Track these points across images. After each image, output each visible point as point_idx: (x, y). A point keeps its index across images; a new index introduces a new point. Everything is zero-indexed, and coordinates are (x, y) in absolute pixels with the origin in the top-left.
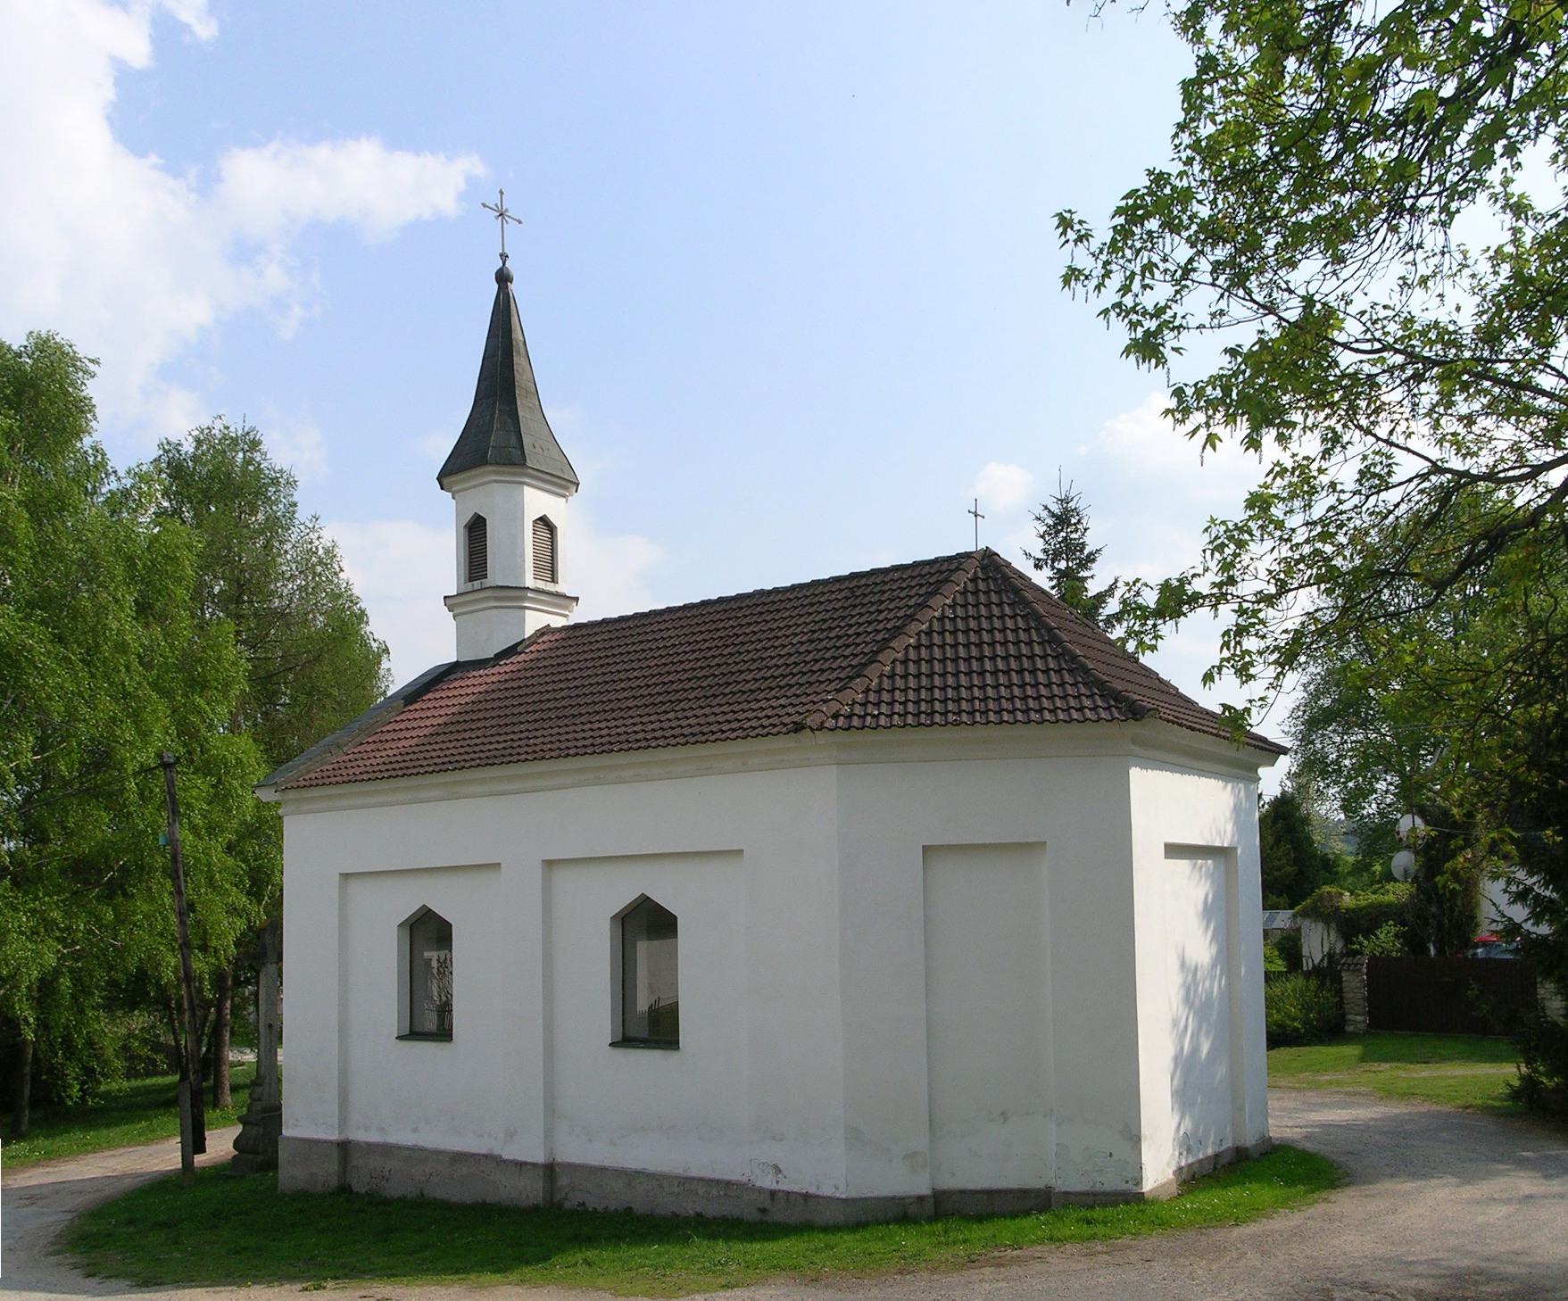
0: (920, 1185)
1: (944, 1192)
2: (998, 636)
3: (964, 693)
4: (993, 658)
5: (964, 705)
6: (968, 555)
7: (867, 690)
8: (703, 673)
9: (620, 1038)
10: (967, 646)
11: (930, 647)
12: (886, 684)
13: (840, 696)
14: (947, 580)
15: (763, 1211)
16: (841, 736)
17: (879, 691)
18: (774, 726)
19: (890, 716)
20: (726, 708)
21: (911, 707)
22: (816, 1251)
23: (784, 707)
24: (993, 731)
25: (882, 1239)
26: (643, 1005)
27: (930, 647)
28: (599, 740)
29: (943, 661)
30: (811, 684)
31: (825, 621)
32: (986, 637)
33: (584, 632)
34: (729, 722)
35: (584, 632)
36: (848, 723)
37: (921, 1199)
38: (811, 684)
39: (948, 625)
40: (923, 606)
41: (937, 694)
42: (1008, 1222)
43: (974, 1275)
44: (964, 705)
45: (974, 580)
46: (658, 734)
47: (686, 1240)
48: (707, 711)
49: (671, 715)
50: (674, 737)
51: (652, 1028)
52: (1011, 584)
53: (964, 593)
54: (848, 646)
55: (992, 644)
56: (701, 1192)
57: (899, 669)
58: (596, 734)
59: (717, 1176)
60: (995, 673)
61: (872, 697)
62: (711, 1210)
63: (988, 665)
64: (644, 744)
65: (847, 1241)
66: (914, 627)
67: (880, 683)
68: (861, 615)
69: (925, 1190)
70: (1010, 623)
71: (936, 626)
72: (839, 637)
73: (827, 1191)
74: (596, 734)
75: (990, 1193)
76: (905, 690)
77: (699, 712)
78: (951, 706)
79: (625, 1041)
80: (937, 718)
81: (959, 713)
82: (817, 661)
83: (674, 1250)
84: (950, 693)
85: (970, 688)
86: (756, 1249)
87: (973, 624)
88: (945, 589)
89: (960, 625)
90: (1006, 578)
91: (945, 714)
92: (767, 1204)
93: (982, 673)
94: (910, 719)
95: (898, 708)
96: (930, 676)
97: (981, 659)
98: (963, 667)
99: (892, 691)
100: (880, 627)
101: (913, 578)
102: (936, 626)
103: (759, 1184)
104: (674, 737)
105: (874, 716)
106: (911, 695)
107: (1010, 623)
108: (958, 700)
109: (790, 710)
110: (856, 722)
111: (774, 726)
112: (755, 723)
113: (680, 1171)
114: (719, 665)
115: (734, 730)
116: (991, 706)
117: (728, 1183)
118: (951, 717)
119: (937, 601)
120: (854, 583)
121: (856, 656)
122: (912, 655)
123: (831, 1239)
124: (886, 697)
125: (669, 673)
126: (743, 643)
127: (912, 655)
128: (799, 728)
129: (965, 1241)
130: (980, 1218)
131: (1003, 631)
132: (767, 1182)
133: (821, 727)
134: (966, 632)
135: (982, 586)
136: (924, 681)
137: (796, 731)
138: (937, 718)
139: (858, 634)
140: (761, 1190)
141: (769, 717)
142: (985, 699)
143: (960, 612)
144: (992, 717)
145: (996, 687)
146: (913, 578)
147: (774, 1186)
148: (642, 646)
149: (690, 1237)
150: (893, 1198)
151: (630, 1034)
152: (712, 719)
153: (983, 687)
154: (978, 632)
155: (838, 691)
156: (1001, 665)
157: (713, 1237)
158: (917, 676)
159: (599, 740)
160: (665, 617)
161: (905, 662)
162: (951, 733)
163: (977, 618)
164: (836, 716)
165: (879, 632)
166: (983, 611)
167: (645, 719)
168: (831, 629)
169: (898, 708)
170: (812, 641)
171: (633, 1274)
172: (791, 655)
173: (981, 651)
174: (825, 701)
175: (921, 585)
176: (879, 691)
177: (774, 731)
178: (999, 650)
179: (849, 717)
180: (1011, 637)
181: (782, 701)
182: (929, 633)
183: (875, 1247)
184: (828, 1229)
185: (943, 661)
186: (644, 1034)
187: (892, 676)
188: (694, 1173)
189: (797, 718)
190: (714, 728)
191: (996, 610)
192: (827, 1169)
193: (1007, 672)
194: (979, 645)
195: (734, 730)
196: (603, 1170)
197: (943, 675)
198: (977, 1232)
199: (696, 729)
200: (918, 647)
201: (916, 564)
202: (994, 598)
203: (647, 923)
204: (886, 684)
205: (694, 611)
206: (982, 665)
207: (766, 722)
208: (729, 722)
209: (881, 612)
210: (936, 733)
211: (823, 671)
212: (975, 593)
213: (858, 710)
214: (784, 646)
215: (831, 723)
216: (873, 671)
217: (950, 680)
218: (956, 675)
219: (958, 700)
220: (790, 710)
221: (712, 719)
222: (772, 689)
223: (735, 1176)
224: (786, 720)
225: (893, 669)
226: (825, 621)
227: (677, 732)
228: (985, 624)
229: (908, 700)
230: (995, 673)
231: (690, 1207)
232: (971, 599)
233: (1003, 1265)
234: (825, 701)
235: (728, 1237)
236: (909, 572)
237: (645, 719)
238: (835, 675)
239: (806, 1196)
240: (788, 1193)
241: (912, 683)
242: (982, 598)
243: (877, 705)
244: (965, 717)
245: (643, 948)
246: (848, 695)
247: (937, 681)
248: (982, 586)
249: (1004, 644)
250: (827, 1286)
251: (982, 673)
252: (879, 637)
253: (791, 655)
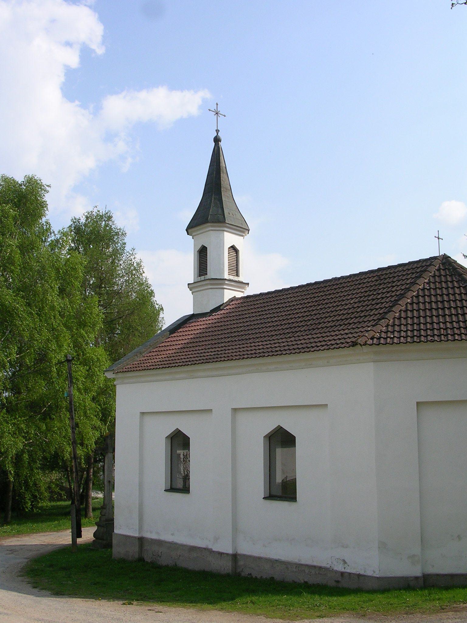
0: (416, 571)
1: (429, 575)
2: (452, 297)
3: (435, 326)
4: (449, 308)
5: (436, 332)
6: (435, 258)
7: (387, 326)
8: (308, 318)
9: (268, 495)
10: (436, 302)
11: (418, 303)
12: (397, 322)
13: (374, 328)
14: (425, 271)
15: (338, 582)
16: (375, 348)
17: (393, 326)
18: (343, 343)
19: (399, 338)
20: (319, 335)
21: (409, 333)
22: (364, 602)
23: (347, 334)
24: (451, 345)
25: (397, 597)
26: (279, 479)
27: (418, 303)
28: (258, 351)
29: (424, 310)
30: (360, 323)
31: (366, 292)
32: (446, 298)
33: (251, 299)
34: (320, 342)
35: (251, 299)
36: (378, 342)
37: (417, 578)
38: (360, 323)
39: (427, 293)
40: (414, 283)
41: (422, 326)
42: (461, 590)
43: (443, 615)
44: (436, 332)
45: (439, 270)
46: (286, 348)
47: (299, 594)
48: (310, 336)
49: (293, 339)
50: (294, 349)
51: (283, 491)
52: (457, 271)
53: (434, 276)
54: (378, 304)
55: (449, 301)
56: (307, 571)
57: (403, 315)
58: (257, 348)
59: (315, 564)
60: (451, 315)
61: (390, 329)
62: (312, 580)
63: (447, 312)
64: (279, 353)
65: (379, 598)
66: (410, 294)
67: (394, 322)
68: (384, 288)
69: (419, 574)
70: (457, 291)
71: (421, 293)
72: (373, 300)
73: (369, 573)
74: (257, 348)
75: (452, 576)
76: (406, 325)
77: (306, 337)
78: (429, 332)
79: (270, 497)
80: (423, 339)
81: (433, 336)
82: (362, 311)
83: (294, 599)
84: (429, 326)
85: (438, 323)
86: (335, 600)
87: (439, 292)
88: (426, 275)
89: (433, 292)
90: (455, 269)
91: (426, 336)
92: (340, 579)
93: (444, 316)
94: (409, 339)
95: (403, 334)
96: (418, 318)
97: (443, 309)
98: (434, 313)
99: (400, 325)
100: (393, 294)
101: (409, 270)
102: (421, 293)
103: (335, 568)
104: (294, 349)
105: (391, 338)
106: (409, 327)
107: (457, 291)
108: (433, 330)
109: (350, 335)
110: (382, 341)
111: (343, 343)
112: (333, 342)
113: (296, 561)
114: (316, 314)
115: (323, 346)
116: (449, 332)
117: (320, 568)
118: (429, 338)
119: (421, 281)
120: (380, 273)
121: (382, 308)
122: (409, 307)
123: (371, 596)
124: (397, 328)
125: (291, 318)
126: (327, 303)
127: (409, 307)
128: (354, 344)
129: (439, 599)
130: (447, 588)
131: (454, 294)
132: (339, 568)
133: (365, 344)
134: (435, 296)
135: (443, 273)
136: (416, 321)
137: (353, 346)
138: (423, 339)
139: (383, 298)
140: (336, 572)
141: (340, 339)
142: (446, 329)
143: (432, 286)
144: (450, 337)
145: (451, 323)
146: (409, 270)
147: (343, 570)
148: (279, 306)
149: (301, 593)
150: (403, 578)
151: (274, 493)
152: (312, 340)
153: (445, 323)
154: (441, 295)
155: (373, 326)
156: (453, 311)
157: (313, 593)
158: (412, 318)
159: (258, 351)
160: (290, 292)
161: (406, 311)
162: (430, 346)
163: (441, 289)
164: (372, 338)
165: (392, 296)
166: (444, 285)
167: (280, 341)
168: (369, 296)
169: (403, 334)
170: (360, 302)
171: (274, 608)
172: (350, 309)
173: (444, 305)
174: (367, 331)
175: (413, 273)
176: (393, 326)
177: (343, 346)
178: (453, 304)
179: (379, 339)
180: (458, 297)
181: (346, 331)
182: (417, 297)
183: (392, 601)
184: (369, 592)
185: (424, 310)
186: (279, 493)
187: (399, 318)
188: (303, 562)
189: (354, 340)
190: (313, 345)
191: (450, 285)
192: (369, 563)
193: (457, 315)
194: (442, 302)
195: (323, 346)
196: (260, 558)
197: (425, 317)
198: (446, 595)
199: (304, 346)
200: (412, 304)
201: (410, 263)
202: (449, 279)
203: (281, 439)
204: (397, 322)
205: (304, 289)
206: (444, 312)
207: (338, 342)
208: (320, 342)
209: (393, 287)
210: (422, 346)
211: (366, 316)
212: (440, 276)
213: (383, 335)
214: (347, 304)
215: (370, 342)
216: (390, 316)
217: (429, 320)
218: (431, 317)
219: (433, 330)
220: (350, 335)
221: (312, 340)
222: (341, 325)
223: (324, 565)
224: (349, 340)
225: (400, 314)
226: (366, 292)
227: (296, 347)
228: (445, 291)
229: (407, 330)
230: (451, 315)
231: (301, 578)
232: (437, 279)
233: (459, 611)
234: (367, 331)
235: (320, 594)
236: (407, 267)
237: (280, 341)
238: (372, 318)
239: (359, 576)
240: (350, 574)
241: (410, 321)
242: (443, 279)
243: (393, 332)
244: (436, 338)
245: (279, 451)
246: (378, 328)
247: (422, 320)
248: (443, 273)
249: (455, 301)
250: (369, 619)
251: (444, 316)
252: (393, 299)
253: (350, 309)
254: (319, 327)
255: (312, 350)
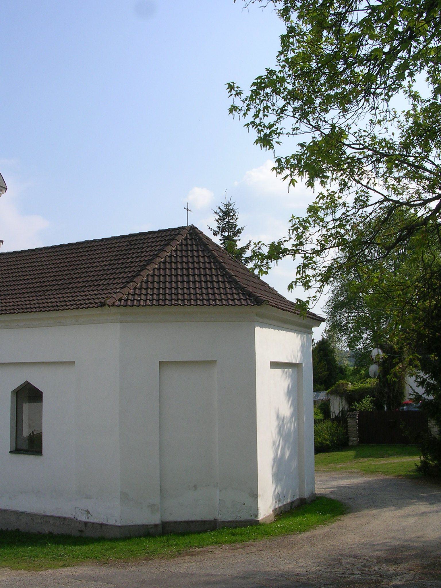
0: (155, 519)
1: (167, 523)
2: (196, 265)
3: (180, 291)
4: (194, 275)
5: (180, 297)
6: (183, 228)
7: (135, 288)
8: (59, 278)
9: (14, 449)
10: (182, 269)
11: (165, 269)
12: (144, 285)
13: (122, 291)
14: (173, 239)
15: (81, 531)
16: (123, 310)
17: (141, 289)
18: (91, 303)
19: (145, 301)
20: (69, 295)
21: (155, 297)
22: (106, 550)
23: (96, 295)
24: (192, 309)
25: (137, 544)
26: (26, 433)
27: (165, 269)
28: (9, 308)
29: (170, 276)
30: (109, 284)
31: (117, 255)
32: (191, 266)
33: (5, 257)
34: (70, 301)
35: (5, 257)
36: (126, 303)
37: (156, 526)
38: (109, 284)
39: (173, 260)
40: (162, 250)
41: (167, 291)
42: (197, 536)
43: (180, 560)
44: (180, 297)
45: (186, 239)
46: (37, 306)
47: (44, 545)
48: (60, 296)
49: (43, 297)
50: (44, 307)
51: (30, 444)
52: (202, 242)
53: (181, 245)
54: (127, 268)
55: (193, 269)
56: (52, 522)
57: (150, 279)
58: (8, 304)
59: (59, 515)
60: (194, 282)
61: (137, 292)
62: (57, 531)
63: (191, 278)
64: (30, 310)
65: (121, 545)
66: (158, 260)
67: (141, 285)
68: (134, 253)
69: (158, 521)
70: (202, 260)
71: (168, 260)
72: (123, 263)
73: (111, 522)
74: (8, 304)
75: (188, 523)
76: (153, 289)
77: (56, 296)
78: (174, 297)
79: (17, 450)
80: (167, 302)
81: (177, 300)
82: (112, 274)
83: (39, 549)
84: (173, 291)
85: (183, 289)
86: (78, 549)
87: (185, 259)
88: (173, 243)
89: (179, 259)
90: (200, 239)
91: (171, 300)
92: (83, 528)
93: (188, 282)
94: (155, 302)
95: (149, 297)
96: (164, 282)
97: (188, 276)
98: (180, 279)
99: (146, 289)
100: (142, 259)
101: (158, 237)
102: (168, 260)
103: (79, 519)
104: (44, 307)
105: (138, 300)
106: (156, 291)
107: (202, 260)
108: (177, 294)
109: (99, 296)
110: (129, 303)
111: (91, 303)
112: (82, 302)
113: (42, 512)
114: (67, 275)
115: (72, 305)
116: (192, 297)
117: (65, 519)
118: (174, 302)
119: (169, 248)
120: (131, 239)
121: (130, 272)
122: (157, 272)
123: (113, 544)
124: (144, 292)
125: (43, 277)
126: (78, 265)
127: (157, 272)
128: (103, 305)
129: (176, 545)
130: (183, 534)
131: (199, 263)
132: (83, 518)
133: (113, 305)
134: (181, 263)
135: (189, 242)
136: (162, 285)
137: (101, 306)
138: (167, 302)
139: (132, 262)
140: (80, 522)
141: (89, 299)
142: (190, 294)
143: (179, 253)
144: (193, 302)
145: (195, 289)
146: (158, 237)
147: (86, 520)
148: (32, 264)
149: (46, 543)
150: (143, 525)
151: (19, 447)
152: (62, 299)
153: (189, 289)
154: (187, 263)
155: (122, 288)
156: (197, 278)
157: (57, 543)
158: (159, 283)
159: (9, 308)
161: (153, 276)
162: (174, 309)
163: (187, 257)
164: (120, 300)
165: (141, 261)
166: (190, 253)
167: (31, 299)
168: (119, 259)
169: (149, 297)
170: (110, 265)
171: (19, 560)
172: (100, 271)
173: (188, 272)
174: (116, 293)
175: (162, 241)
176: (141, 289)
177: (91, 306)
178: (197, 272)
179: (126, 300)
180: (202, 266)
181: (95, 292)
182: (165, 263)
183: (133, 548)
184: (111, 540)
185: (170, 276)
186: (25, 446)
187: (147, 282)
188: (48, 514)
189: (102, 300)
190: (63, 304)
191: (195, 254)
192: (110, 511)
193: (200, 282)
194: (187, 269)
195: (72, 305)
196: (6, 511)
197: (170, 282)
198: (182, 540)
199: (55, 304)
200: (159, 269)
201: (160, 231)
202: (195, 248)
203: (28, 395)
204: (144, 285)
205: (57, 249)
206: (189, 278)
207: (87, 302)
208: (70, 301)
209: (142, 252)
210: (167, 309)
211: (115, 279)
212: (186, 245)
213: (131, 297)
214: (97, 267)
215: (118, 303)
216: (138, 279)
217: (174, 285)
218: (176, 283)
219: (177, 294)
220: (99, 296)
221: (62, 299)
222: (91, 286)
223: (68, 515)
224: (97, 301)
225: (147, 279)
226: (117, 255)
227: (46, 305)
228: (190, 260)
229: (154, 294)
230: (194, 282)
231: (46, 529)
232: (184, 248)
233: (194, 555)
234: (116, 293)
235: (64, 544)
236: (156, 234)
237: (31, 299)
238: (120, 281)
239: (102, 525)
240: (93, 523)
241: (156, 285)
242: (189, 248)
243: (140, 295)
244: (180, 302)
245: (26, 407)
246: (126, 290)
247: (168, 285)
248: (189, 242)
249: (199, 269)
250: (111, 566)
251: (188, 282)
252: (141, 264)
253: (100, 271)
254: (53, 288)
255: (43, 309)
